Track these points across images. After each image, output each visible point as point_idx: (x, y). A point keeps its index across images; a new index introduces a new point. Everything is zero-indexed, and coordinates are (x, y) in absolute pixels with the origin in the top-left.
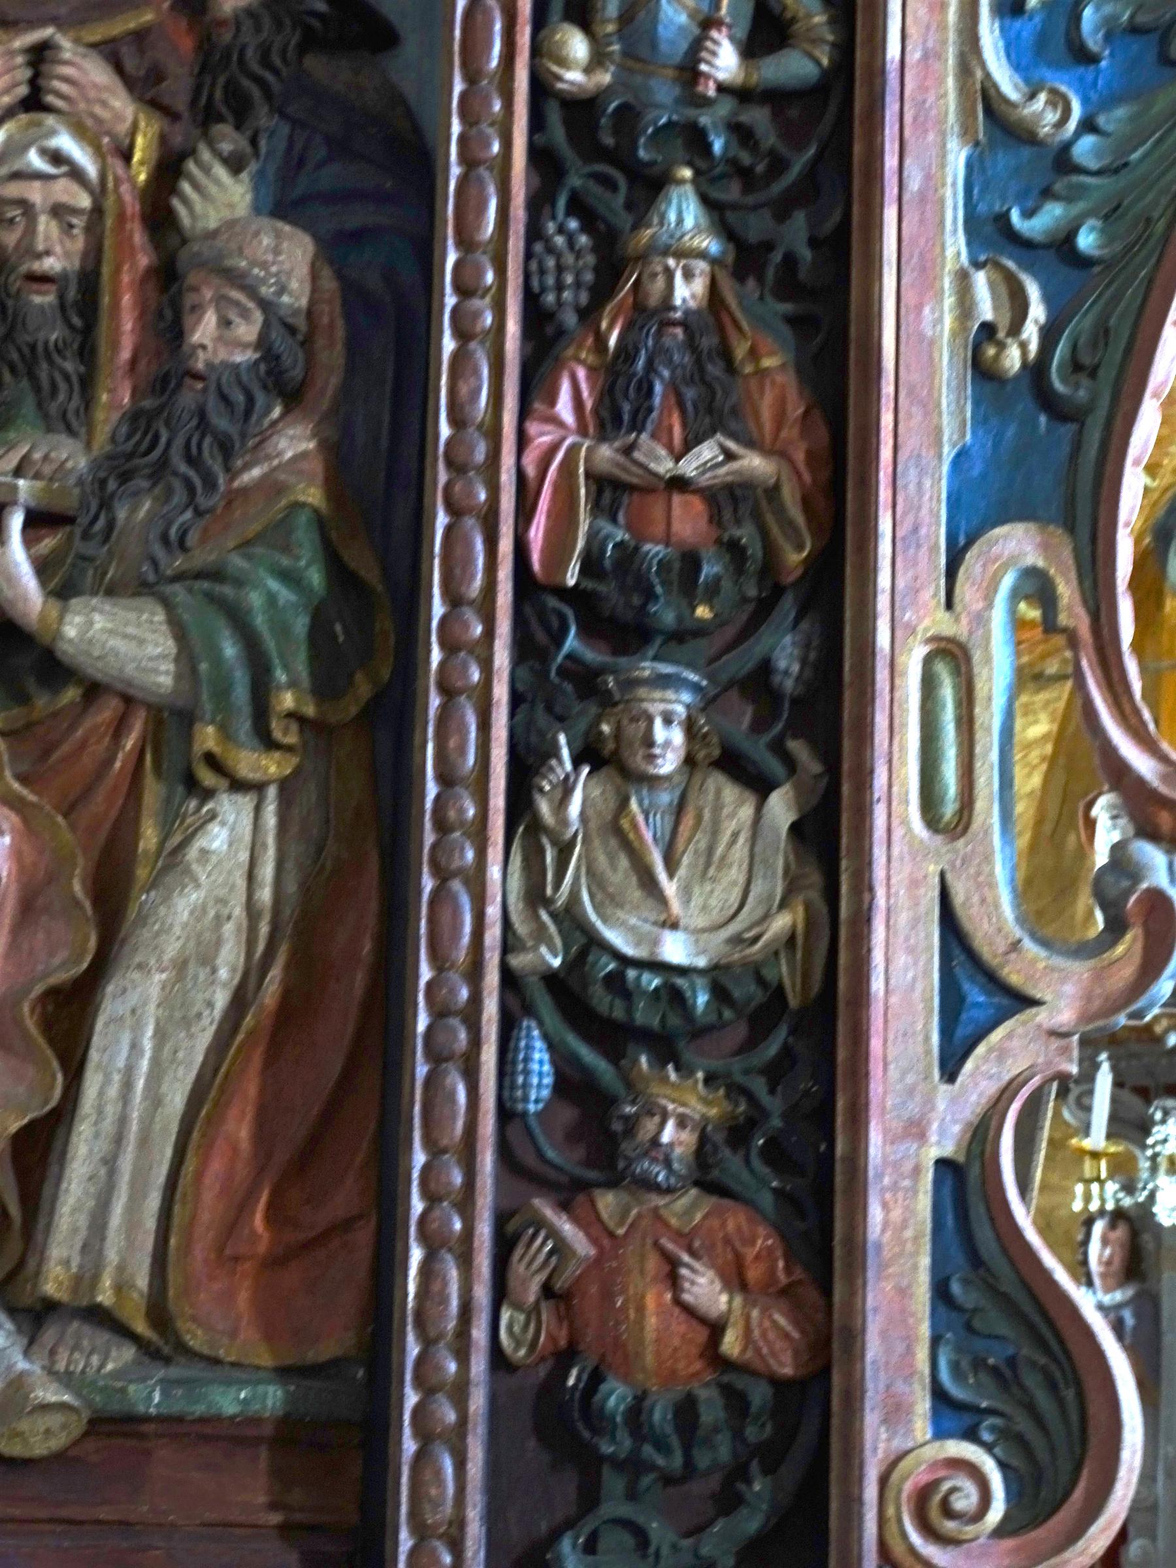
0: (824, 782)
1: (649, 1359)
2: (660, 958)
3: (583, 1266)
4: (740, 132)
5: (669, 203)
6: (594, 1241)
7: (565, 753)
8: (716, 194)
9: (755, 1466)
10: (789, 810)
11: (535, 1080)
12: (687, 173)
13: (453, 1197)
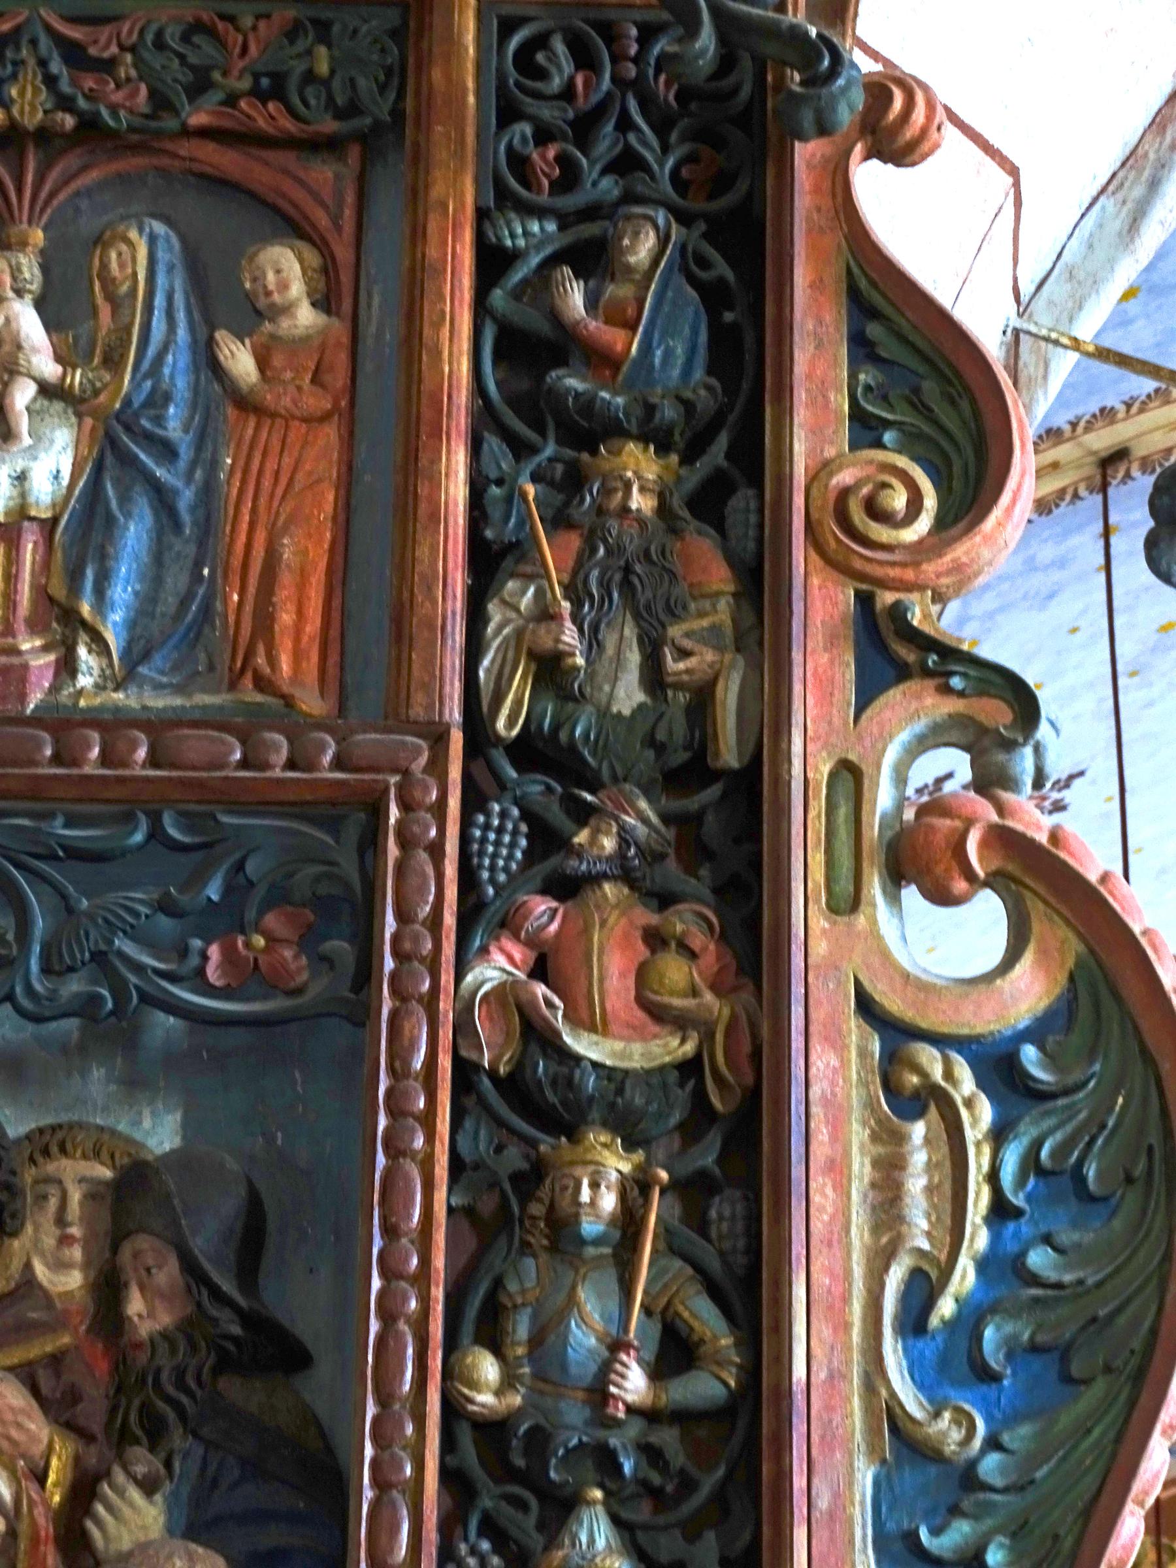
4: (650, 1453)
5: (581, 1524)
8: (625, 1515)
12: (598, 1494)
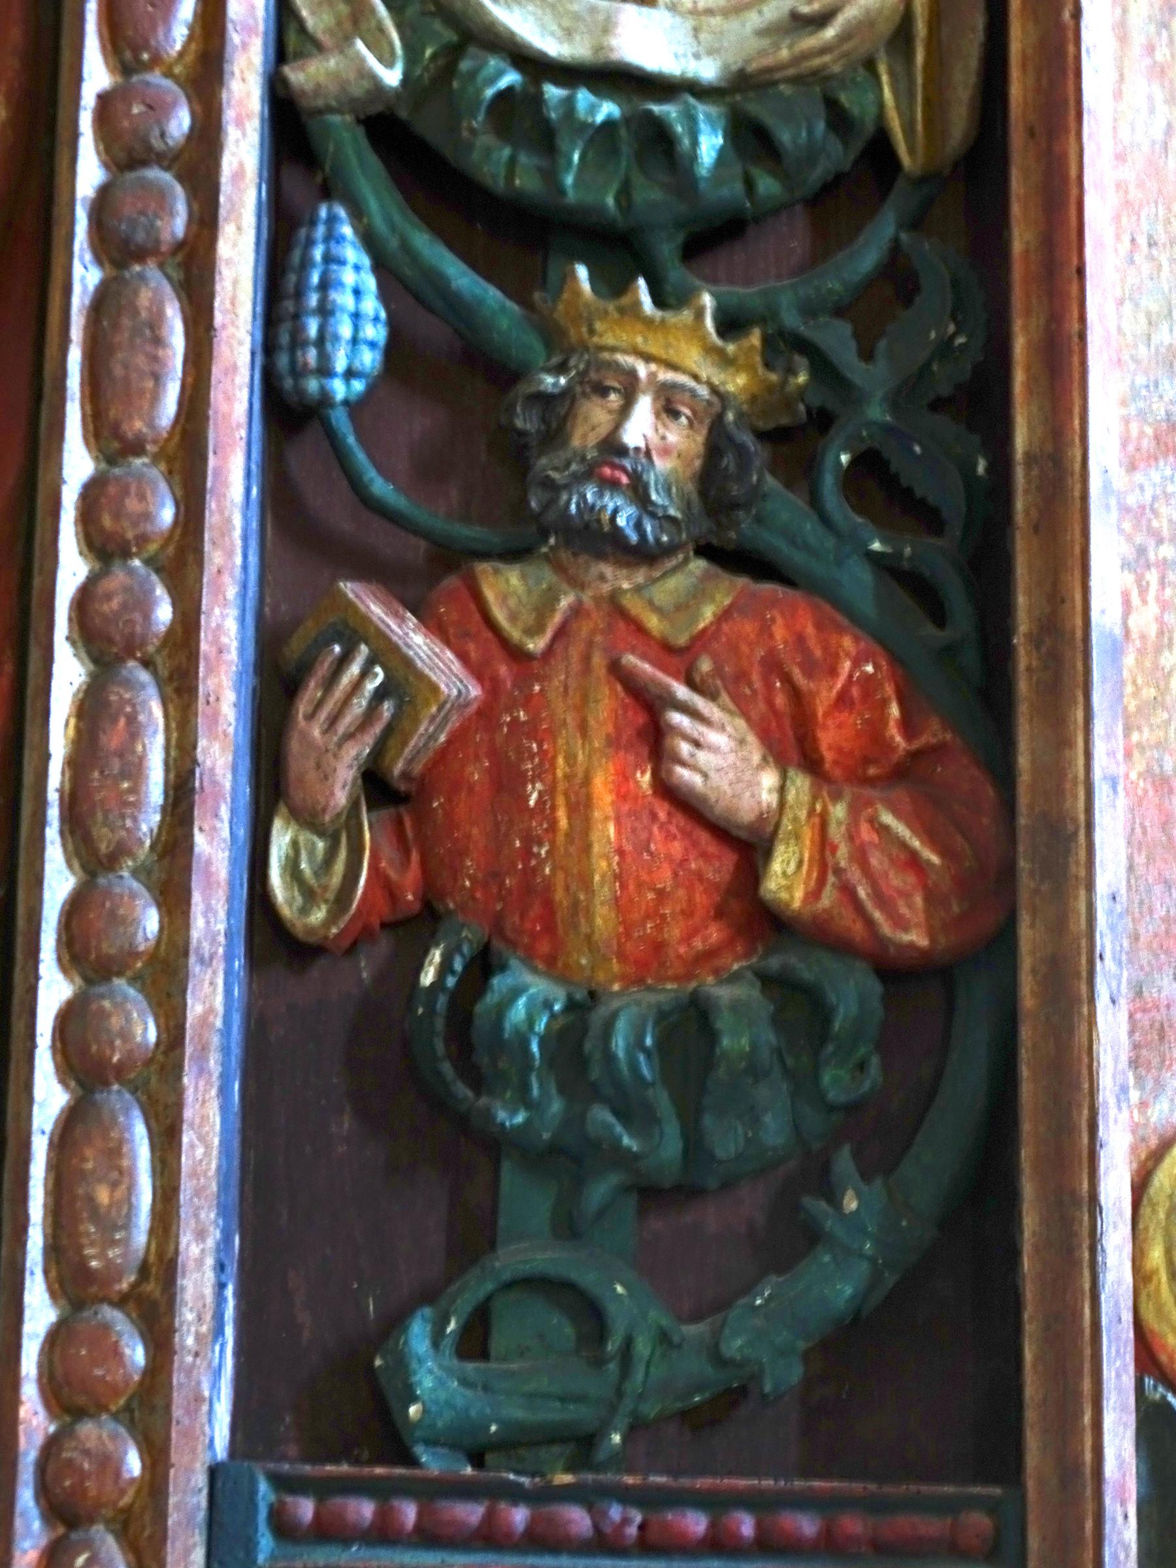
1: (603, 919)
2: (615, 56)
3: (454, 722)
6: (478, 670)
9: (844, 1162)
11: (345, 330)
13: (152, 548)
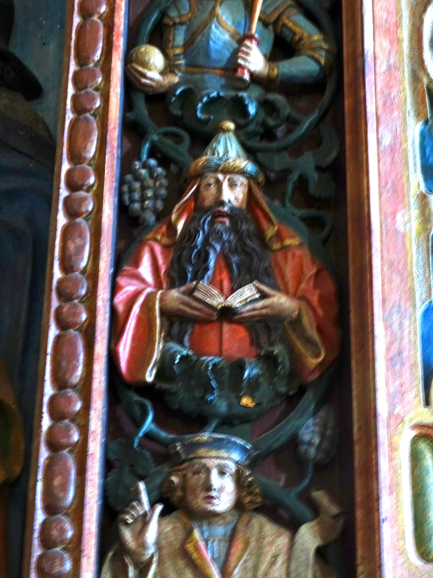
0: (341, 522)
5: (219, 142)
7: (144, 497)
8: (249, 143)
10: (315, 537)
12: (231, 125)
